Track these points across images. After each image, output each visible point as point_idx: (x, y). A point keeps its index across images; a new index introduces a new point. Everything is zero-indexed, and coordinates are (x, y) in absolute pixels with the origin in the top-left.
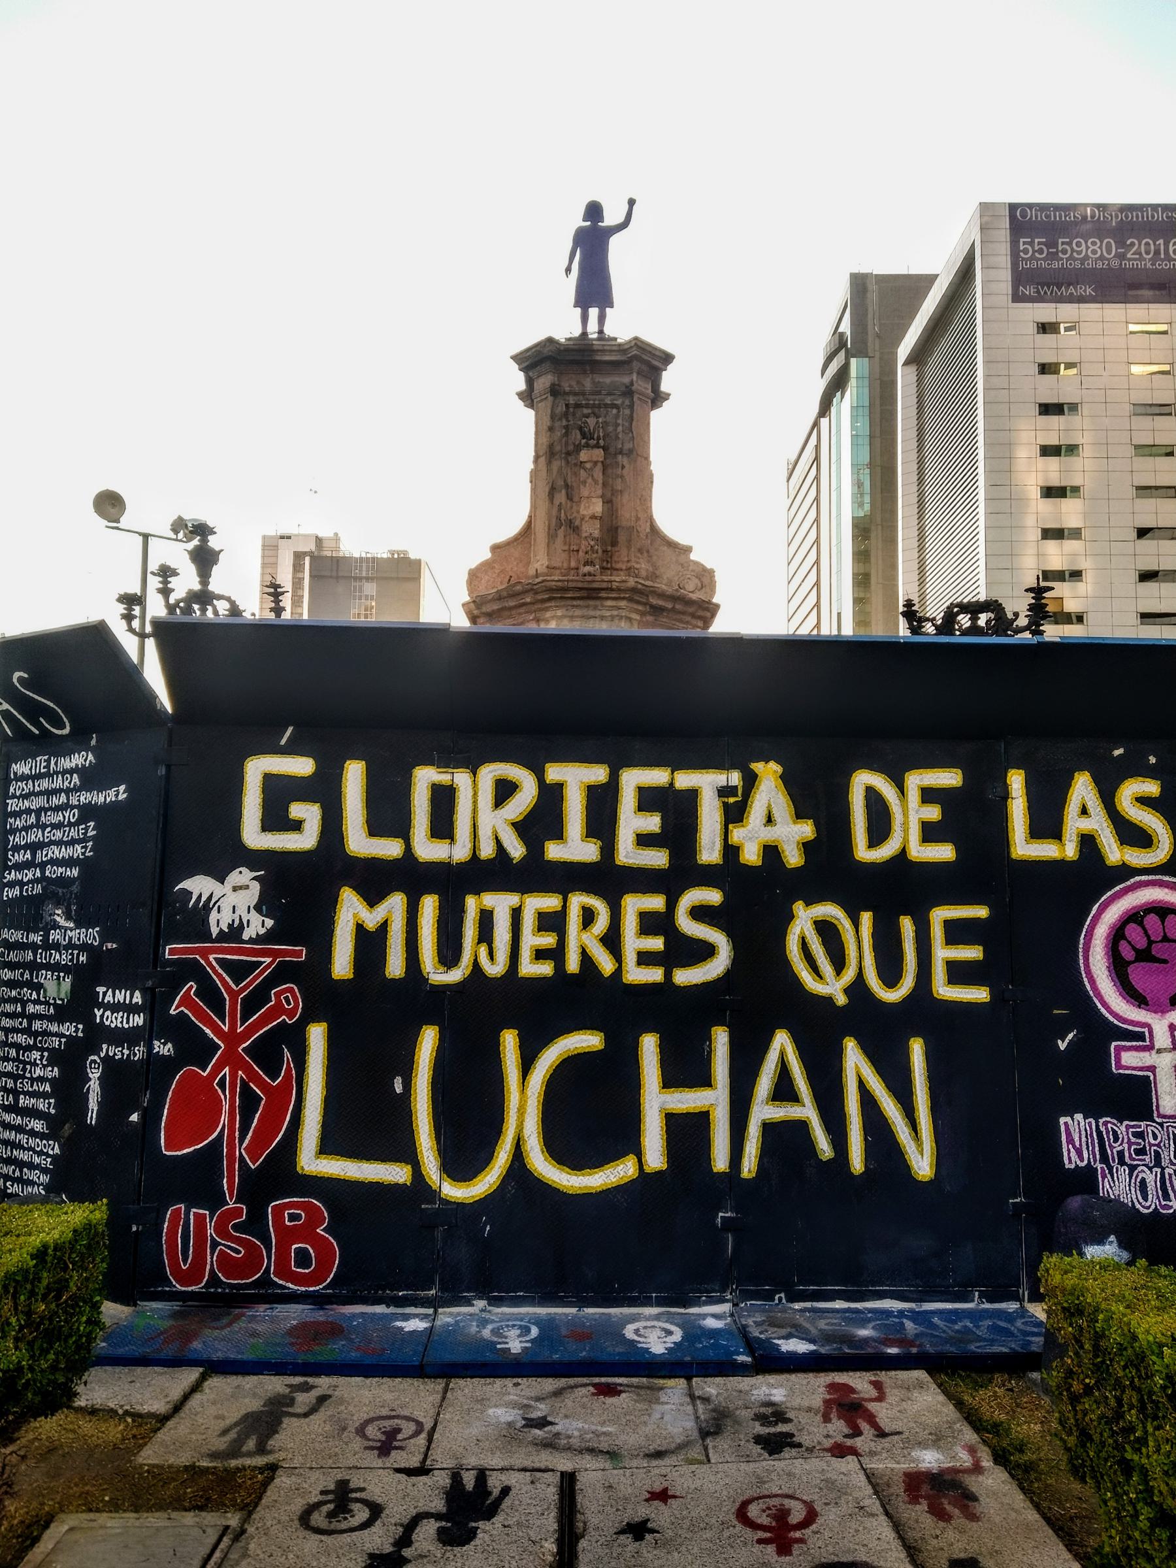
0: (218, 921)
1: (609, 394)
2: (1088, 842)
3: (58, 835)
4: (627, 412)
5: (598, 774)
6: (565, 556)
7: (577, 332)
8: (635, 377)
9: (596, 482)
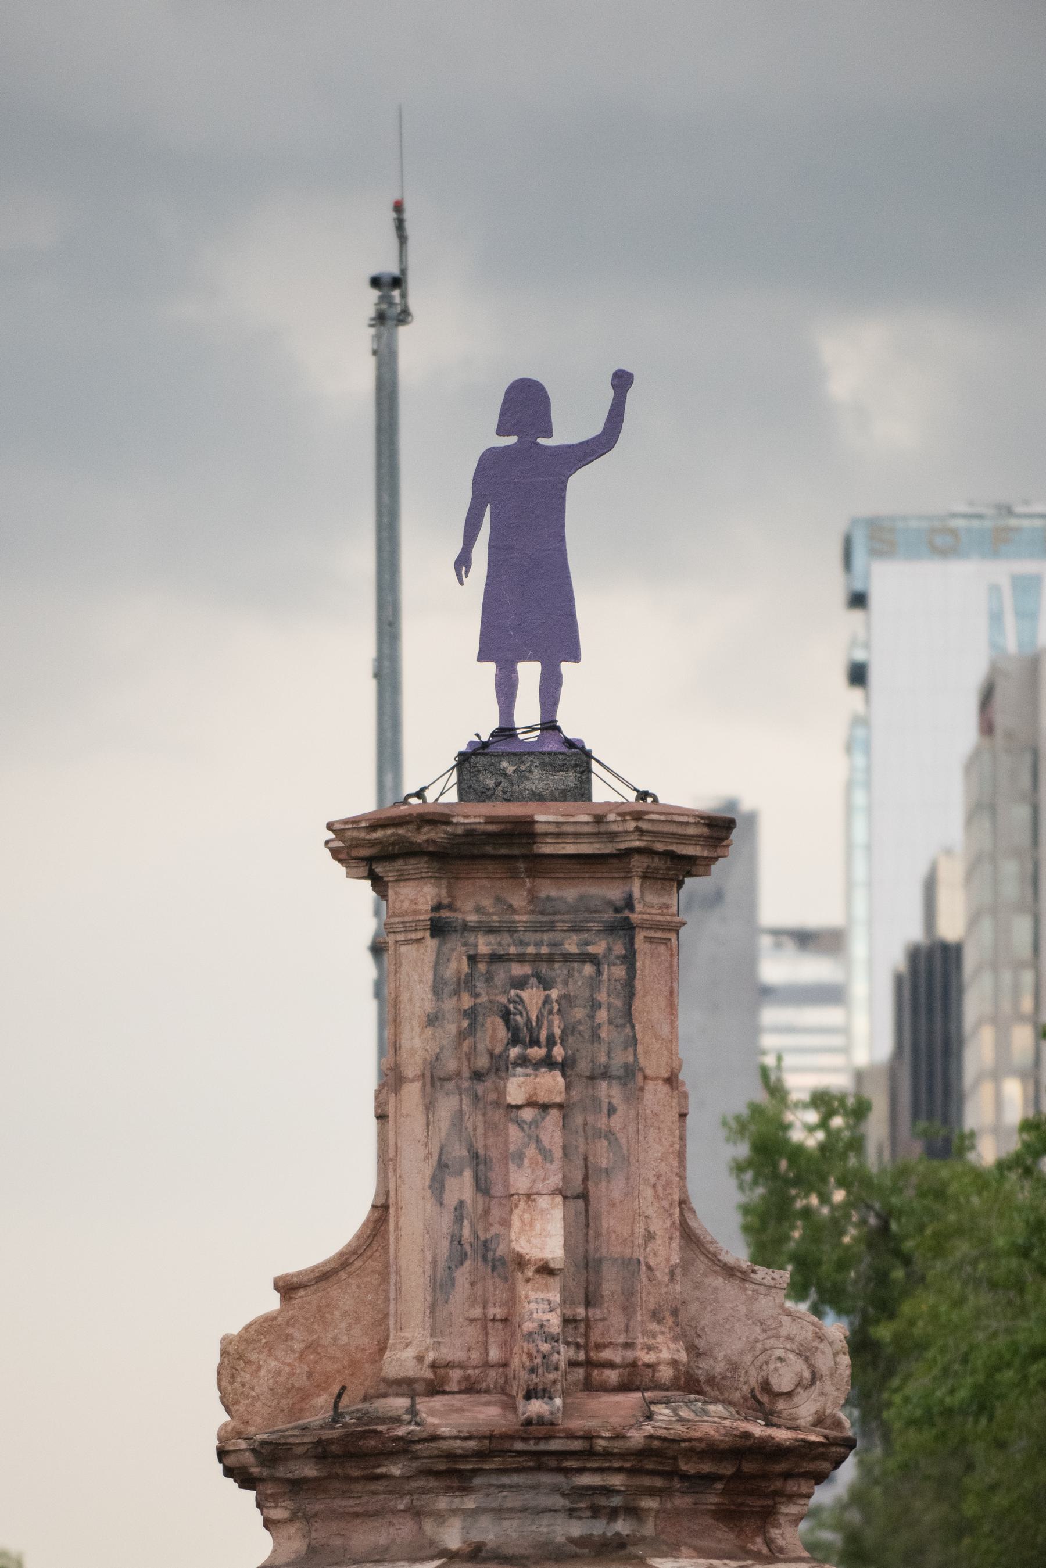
1: (575, 929)
4: (620, 971)
6: (472, 1332)
7: (487, 724)
8: (636, 887)
9: (546, 1155)
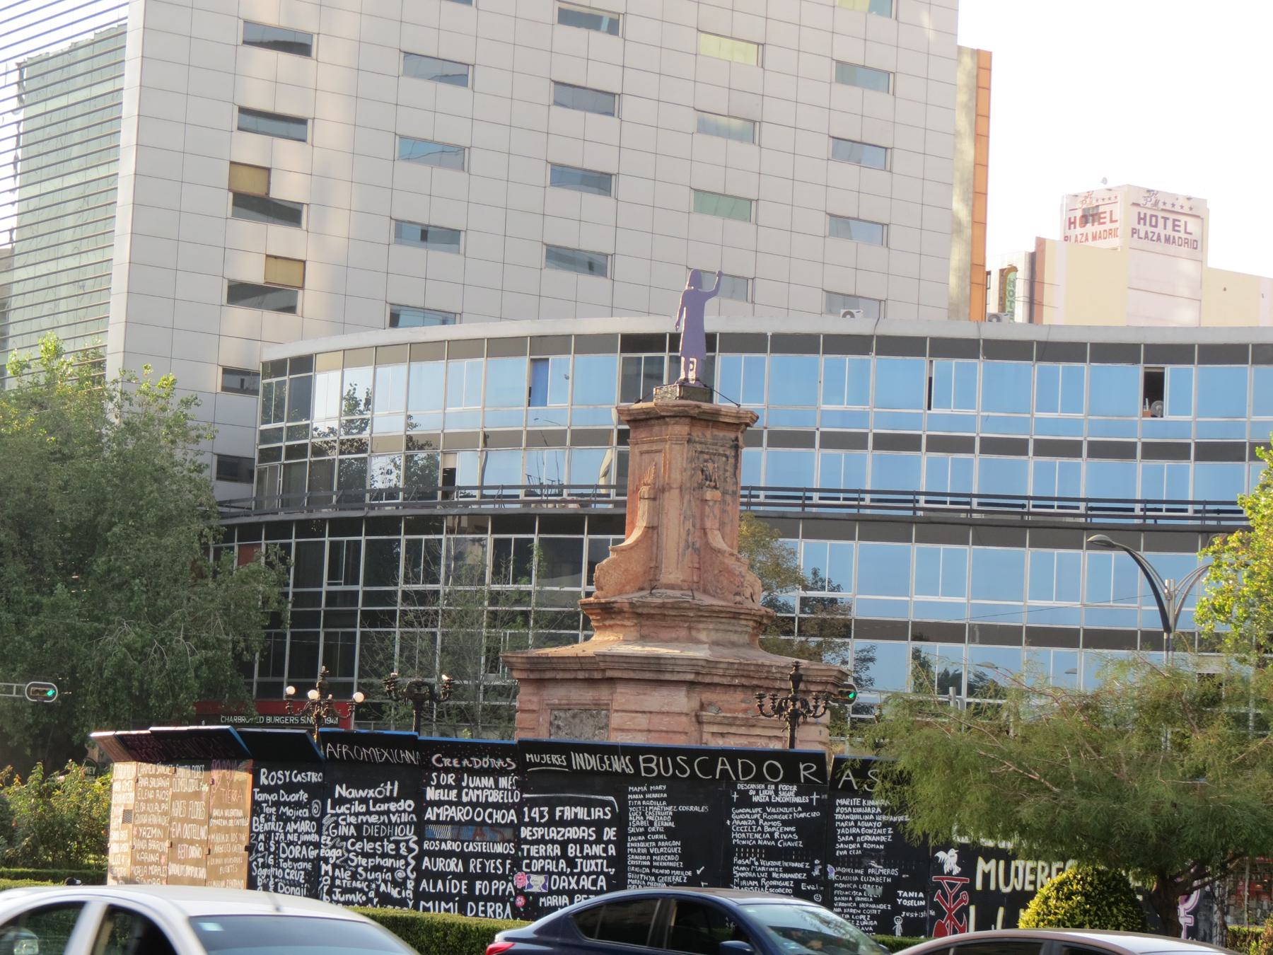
0: (946, 869)
3: (870, 831)
9: (715, 517)
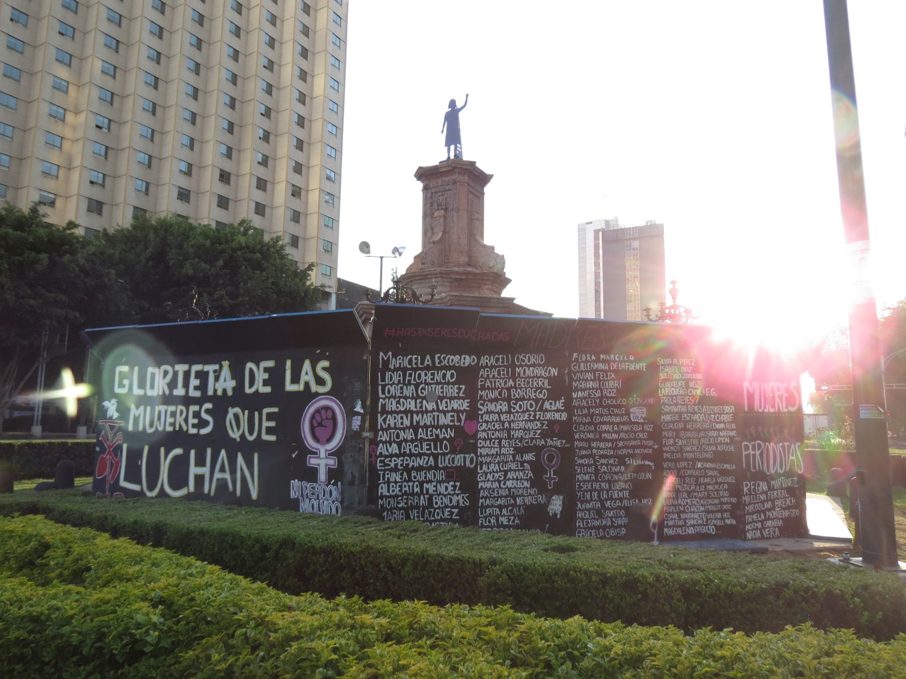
0: (109, 414)
1: (448, 185)
2: (307, 384)
5: (185, 367)
7: (445, 158)
